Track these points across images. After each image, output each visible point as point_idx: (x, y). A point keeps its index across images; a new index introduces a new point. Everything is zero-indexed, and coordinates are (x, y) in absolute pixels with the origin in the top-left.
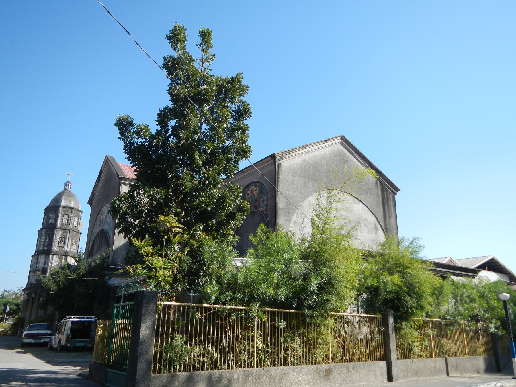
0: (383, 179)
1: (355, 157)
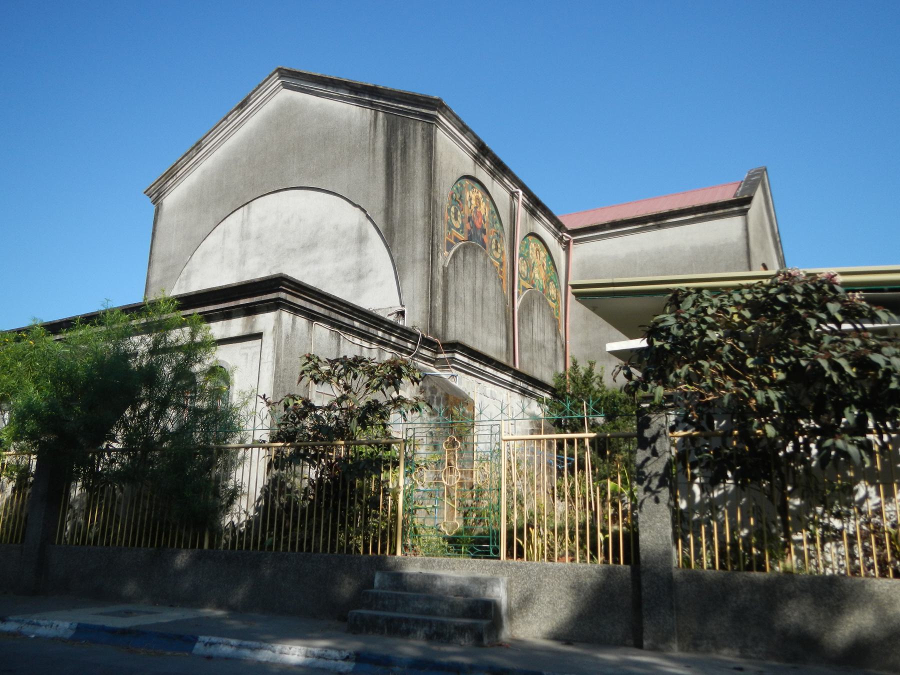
0: (389, 100)
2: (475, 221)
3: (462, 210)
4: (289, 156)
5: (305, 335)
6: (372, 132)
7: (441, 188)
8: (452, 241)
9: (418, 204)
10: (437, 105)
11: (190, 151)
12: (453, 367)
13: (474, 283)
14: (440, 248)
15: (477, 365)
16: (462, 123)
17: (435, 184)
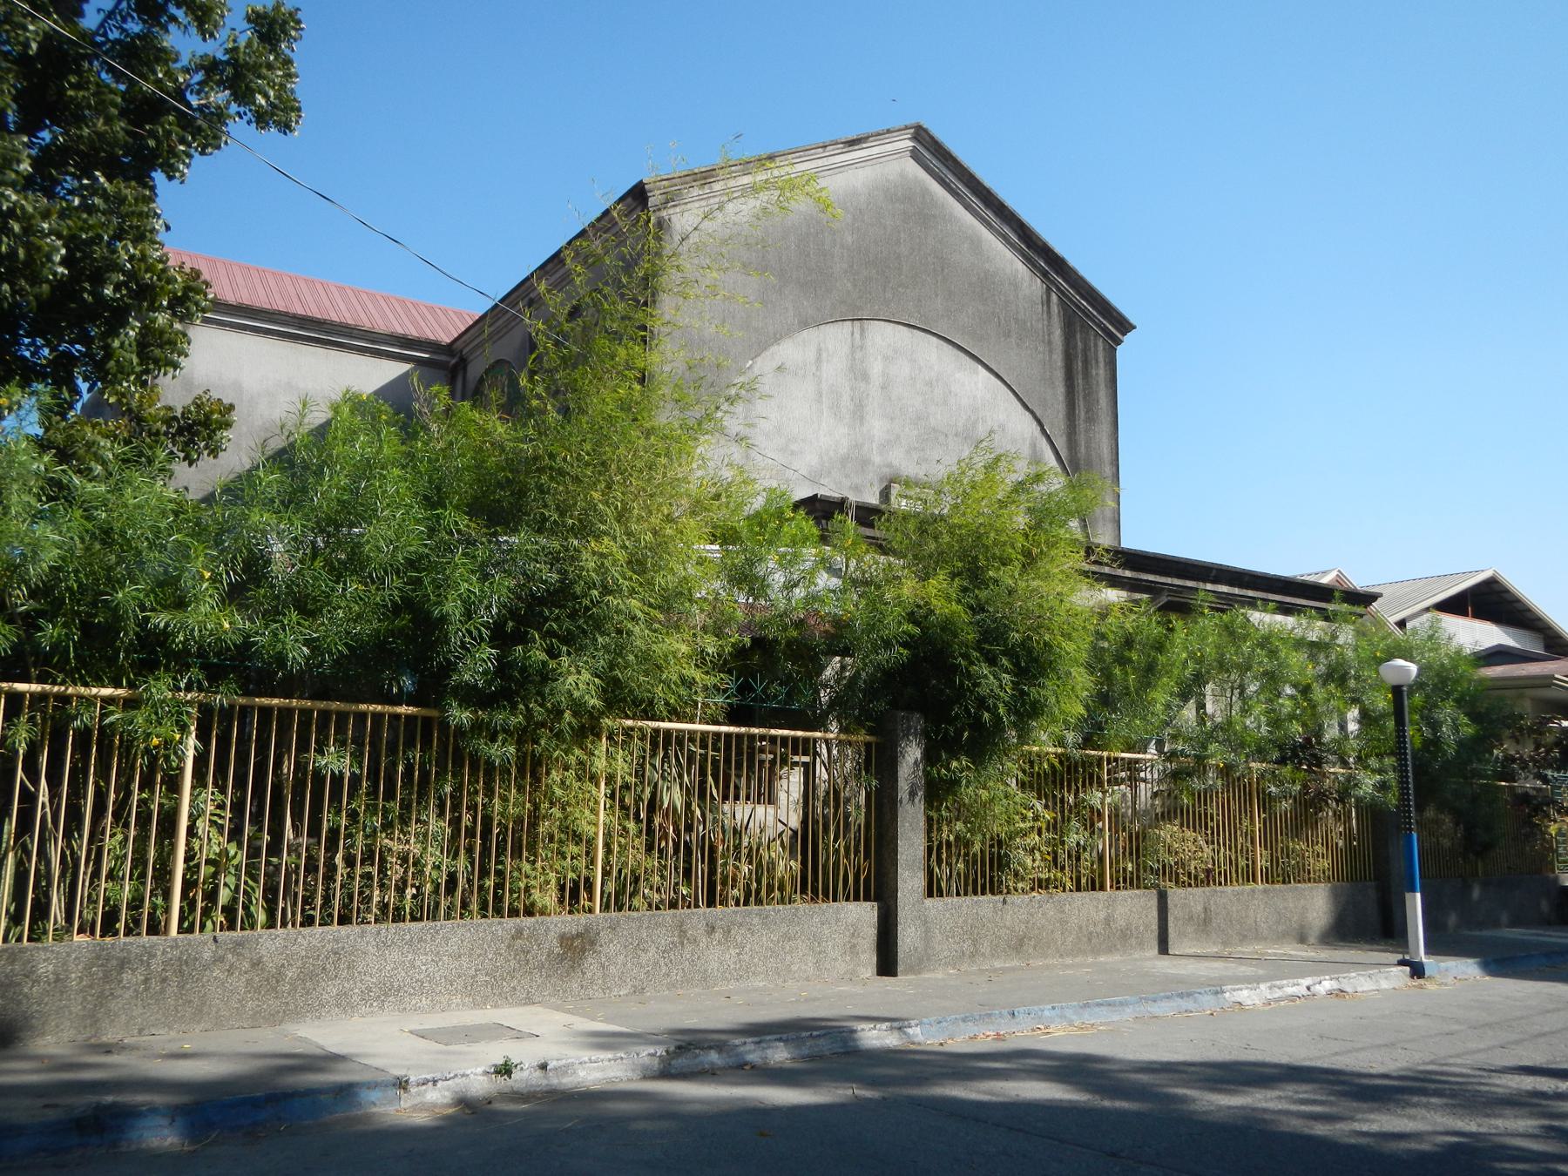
1: (967, 207)
6: (1045, 316)
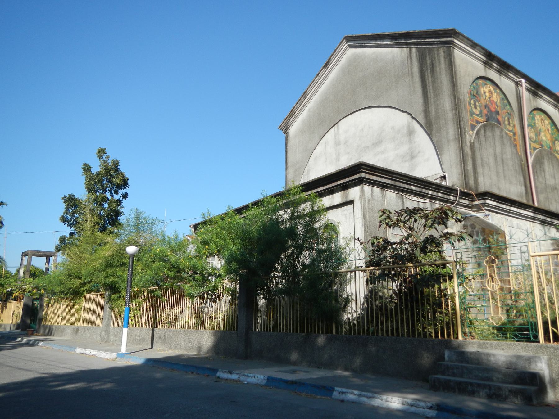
0: (418, 38)
1: (371, 47)
2: (490, 107)
3: (479, 101)
4: (358, 89)
5: (380, 198)
6: (409, 62)
7: (462, 89)
8: (474, 123)
9: (446, 103)
10: (453, 33)
11: (301, 99)
12: (486, 209)
13: (495, 150)
14: (466, 129)
15: (504, 206)
16: (472, 41)
17: (458, 86)
